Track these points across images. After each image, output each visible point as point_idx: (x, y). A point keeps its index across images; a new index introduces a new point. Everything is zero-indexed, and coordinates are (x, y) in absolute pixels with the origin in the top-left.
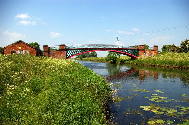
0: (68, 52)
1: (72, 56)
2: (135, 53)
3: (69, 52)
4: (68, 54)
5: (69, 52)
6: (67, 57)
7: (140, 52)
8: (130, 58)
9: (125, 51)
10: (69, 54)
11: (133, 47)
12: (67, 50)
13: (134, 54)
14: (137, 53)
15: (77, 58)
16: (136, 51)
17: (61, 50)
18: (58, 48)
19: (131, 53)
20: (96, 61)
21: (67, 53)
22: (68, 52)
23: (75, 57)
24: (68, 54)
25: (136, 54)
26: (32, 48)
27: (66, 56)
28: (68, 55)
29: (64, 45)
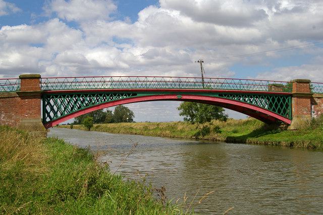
0: (49, 103)
1: (63, 117)
2: (282, 106)
3: (56, 103)
4: (52, 109)
5: (56, 103)
6: (48, 120)
7: (297, 104)
8: (259, 124)
9: (246, 103)
10: (55, 108)
11: (270, 86)
12: (46, 95)
13: (279, 111)
14: (287, 106)
15: (75, 123)
16: (284, 100)
17: (23, 95)
18: (14, 83)
19: (262, 106)
20: (130, 131)
21: (48, 108)
22: (52, 102)
23: (71, 120)
24: (52, 109)
25: (285, 111)
26: (305, 84)
27: (44, 119)
28: (52, 114)
29: (308, 82)
